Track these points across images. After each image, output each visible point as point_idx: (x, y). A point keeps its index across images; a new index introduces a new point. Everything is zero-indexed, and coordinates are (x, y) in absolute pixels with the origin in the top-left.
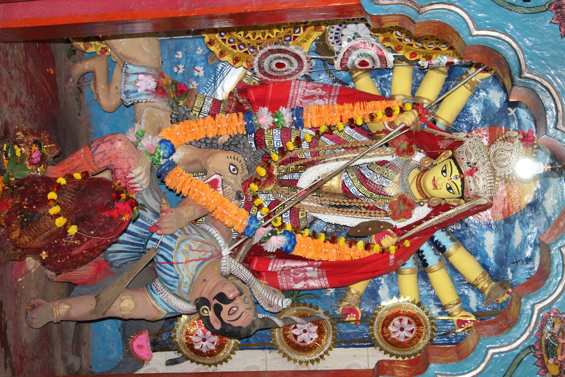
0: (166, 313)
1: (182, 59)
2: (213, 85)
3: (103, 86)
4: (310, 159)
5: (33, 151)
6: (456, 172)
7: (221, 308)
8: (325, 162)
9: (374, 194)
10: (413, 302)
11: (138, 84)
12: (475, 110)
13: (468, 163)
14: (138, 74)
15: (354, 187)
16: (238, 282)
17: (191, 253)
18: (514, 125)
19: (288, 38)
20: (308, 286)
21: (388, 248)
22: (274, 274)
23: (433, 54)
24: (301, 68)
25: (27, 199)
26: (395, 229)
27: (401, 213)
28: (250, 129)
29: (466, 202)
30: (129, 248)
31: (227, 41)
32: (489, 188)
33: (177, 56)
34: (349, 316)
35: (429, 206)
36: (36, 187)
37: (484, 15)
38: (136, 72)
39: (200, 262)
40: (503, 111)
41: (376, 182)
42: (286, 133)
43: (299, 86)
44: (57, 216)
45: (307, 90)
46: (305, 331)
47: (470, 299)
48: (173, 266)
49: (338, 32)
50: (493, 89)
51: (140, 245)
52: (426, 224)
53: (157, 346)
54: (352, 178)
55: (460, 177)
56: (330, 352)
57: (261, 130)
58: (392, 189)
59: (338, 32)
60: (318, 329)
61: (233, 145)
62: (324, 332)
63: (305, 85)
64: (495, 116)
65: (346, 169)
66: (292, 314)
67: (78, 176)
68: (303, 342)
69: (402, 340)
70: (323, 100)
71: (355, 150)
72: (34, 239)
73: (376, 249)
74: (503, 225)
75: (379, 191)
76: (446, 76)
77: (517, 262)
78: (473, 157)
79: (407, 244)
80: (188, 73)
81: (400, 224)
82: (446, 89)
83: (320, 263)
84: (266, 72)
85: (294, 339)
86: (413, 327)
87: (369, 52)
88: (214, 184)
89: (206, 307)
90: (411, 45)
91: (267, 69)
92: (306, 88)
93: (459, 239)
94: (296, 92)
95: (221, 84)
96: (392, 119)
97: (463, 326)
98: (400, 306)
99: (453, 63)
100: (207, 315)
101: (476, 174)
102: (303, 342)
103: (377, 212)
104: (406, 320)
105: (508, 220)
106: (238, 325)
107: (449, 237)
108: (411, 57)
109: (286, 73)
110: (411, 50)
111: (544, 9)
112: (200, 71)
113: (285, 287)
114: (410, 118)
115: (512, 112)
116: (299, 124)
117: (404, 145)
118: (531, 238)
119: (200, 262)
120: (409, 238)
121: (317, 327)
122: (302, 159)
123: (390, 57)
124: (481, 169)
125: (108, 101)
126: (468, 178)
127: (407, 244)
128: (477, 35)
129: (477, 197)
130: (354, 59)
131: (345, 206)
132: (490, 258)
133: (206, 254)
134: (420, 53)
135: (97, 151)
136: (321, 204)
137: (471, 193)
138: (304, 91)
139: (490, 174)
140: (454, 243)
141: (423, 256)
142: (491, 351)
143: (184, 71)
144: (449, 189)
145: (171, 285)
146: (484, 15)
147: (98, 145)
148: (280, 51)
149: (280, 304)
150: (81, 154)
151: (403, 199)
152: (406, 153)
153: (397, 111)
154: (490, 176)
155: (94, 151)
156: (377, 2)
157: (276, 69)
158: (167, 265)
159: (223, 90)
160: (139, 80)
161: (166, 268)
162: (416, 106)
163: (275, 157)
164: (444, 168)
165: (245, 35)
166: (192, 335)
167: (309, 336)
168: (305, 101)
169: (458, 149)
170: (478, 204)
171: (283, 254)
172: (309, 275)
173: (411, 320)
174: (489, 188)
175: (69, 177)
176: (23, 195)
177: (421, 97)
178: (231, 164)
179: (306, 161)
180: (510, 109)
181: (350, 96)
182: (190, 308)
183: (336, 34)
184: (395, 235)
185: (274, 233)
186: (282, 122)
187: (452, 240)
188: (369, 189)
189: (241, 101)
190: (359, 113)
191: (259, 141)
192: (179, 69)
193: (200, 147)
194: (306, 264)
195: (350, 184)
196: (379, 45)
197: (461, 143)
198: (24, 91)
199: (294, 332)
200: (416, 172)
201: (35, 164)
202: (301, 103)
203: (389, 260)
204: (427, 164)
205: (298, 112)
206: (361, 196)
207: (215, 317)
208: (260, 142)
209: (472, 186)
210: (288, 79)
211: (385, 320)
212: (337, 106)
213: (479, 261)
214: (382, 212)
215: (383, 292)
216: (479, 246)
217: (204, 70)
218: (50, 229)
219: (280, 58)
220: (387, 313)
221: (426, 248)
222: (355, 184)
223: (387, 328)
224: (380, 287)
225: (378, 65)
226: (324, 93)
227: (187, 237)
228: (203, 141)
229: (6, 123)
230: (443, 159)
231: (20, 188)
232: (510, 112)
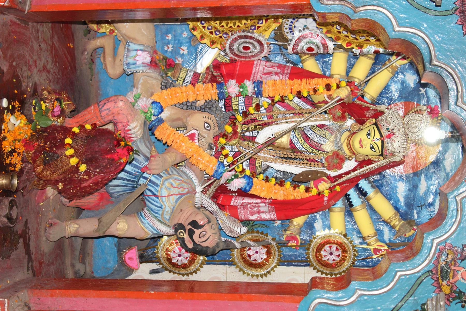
0: (151, 234)
2: (194, 61)
3: (110, 59)
5: (55, 106)
7: (194, 232)
8: (277, 124)
9: (314, 150)
11: (136, 58)
12: (395, 89)
13: (387, 129)
14: (137, 50)
16: (207, 213)
17: (172, 189)
18: (424, 101)
19: (253, 28)
20: (261, 218)
21: (323, 191)
22: (235, 207)
23: (364, 44)
25: (49, 143)
26: (329, 177)
27: (334, 165)
28: (221, 96)
29: (384, 159)
30: (126, 183)
31: (206, 28)
32: (403, 149)
33: (167, 38)
34: (291, 242)
35: (356, 161)
36: (56, 134)
37: (405, 16)
39: (179, 196)
40: (416, 90)
41: (316, 140)
42: (248, 100)
43: (260, 64)
44: (72, 156)
45: (266, 68)
46: (257, 252)
47: (385, 233)
49: (291, 24)
50: (408, 72)
51: (133, 181)
52: (353, 174)
53: (143, 259)
55: (381, 139)
56: (275, 269)
57: (230, 97)
58: (328, 147)
59: (291, 24)
60: (267, 251)
61: (207, 107)
62: (271, 254)
63: (264, 64)
64: (409, 94)
65: (293, 129)
66: (247, 239)
67: (88, 127)
69: (331, 262)
71: (301, 115)
72: (53, 173)
73: (314, 192)
74: (412, 177)
75: (318, 148)
76: (374, 62)
77: (421, 206)
78: (392, 125)
79: (338, 189)
80: (176, 52)
82: (372, 71)
83: (270, 201)
84: (235, 53)
85: (248, 258)
86: (340, 252)
87: (315, 41)
88: (192, 137)
89: (182, 231)
90: (348, 37)
91: (236, 51)
92: (266, 66)
93: (378, 187)
94: (257, 69)
96: (330, 93)
97: (378, 253)
98: (330, 236)
99: (379, 51)
101: (393, 137)
102: (255, 260)
103: (316, 163)
104: (334, 247)
105: (416, 174)
106: (206, 246)
107: (370, 185)
108: (347, 46)
109: (250, 54)
110: (347, 40)
111: (451, 13)
112: (184, 50)
113: (243, 218)
114: (344, 93)
115: (423, 91)
116: (259, 94)
117: (339, 113)
118: (433, 188)
119: (179, 196)
120: (339, 185)
121: (266, 249)
122: (260, 120)
123: (331, 45)
124: (397, 134)
125: (113, 70)
126: (387, 140)
127: (338, 189)
128: (399, 31)
129: (393, 155)
130: (303, 45)
131: (291, 158)
132: (401, 202)
134: (354, 43)
135: (103, 109)
136: (273, 156)
138: (264, 69)
139: (404, 138)
140: (374, 190)
141: (350, 199)
142: (399, 274)
143: (172, 50)
144: (372, 148)
145: (156, 213)
146: (405, 16)
147: (105, 104)
148: (246, 37)
149: (239, 231)
150: (92, 110)
151: (336, 154)
152: (340, 119)
153: (335, 86)
154: (404, 139)
156: (322, 2)
157: (243, 51)
158: (154, 198)
159: (202, 65)
160: (137, 55)
161: (153, 200)
162: (349, 83)
163: (240, 118)
164: (369, 132)
165: (220, 24)
166: (170, 251)
167: (260, 256)
168: (264, 76)
169: (380, 118)
170: (393, 160)
171: (242, 193)
172: (261, 209)
173: (338, 247)
174: (403, 149)
175: (82, 127)
176: (46, 139)
177: (353, 77)
179: (263, 122)
180: (421, 89)
181: (298, 73)
182: (170, 231)
183: (290, 25)
184: (329, 182)
185: (236, 176)
186: (246, 92)
189: (215, 74)
190: (305, 87)
191: (228, 105)
192: (168, 48)
193: (182, 109)
194: (259, 201)
195: (296, 141)
196: (323, 35)
197: (382, 113)
198: (50, 60)
199: (249, 252)
200: (347, 134)
201: (56, 116)
202: (261, 77)
203: (323, 201)
204: (356, 128)
205: (259, 84)
206: (304, 151)
208: (228, 107)
209: (390, 146)
210: (252, 59)
211: (319, 246)
212: (288, 81)
213: (392, 204)
215: (318, 225)
216: (393, 193)
217: (187, 49)
218: (66, 166)
219: (246, 42)
220: (320, 241)
221: (352, 193)
222: (300, 141)
223: (320, 252)
224: (316, 221)
225: (322, 51)
226: (279, 71)
227: (170, 176)
228: (184, 104)
229: (35, 84)
231: (44, 134)
232: (421, 91)
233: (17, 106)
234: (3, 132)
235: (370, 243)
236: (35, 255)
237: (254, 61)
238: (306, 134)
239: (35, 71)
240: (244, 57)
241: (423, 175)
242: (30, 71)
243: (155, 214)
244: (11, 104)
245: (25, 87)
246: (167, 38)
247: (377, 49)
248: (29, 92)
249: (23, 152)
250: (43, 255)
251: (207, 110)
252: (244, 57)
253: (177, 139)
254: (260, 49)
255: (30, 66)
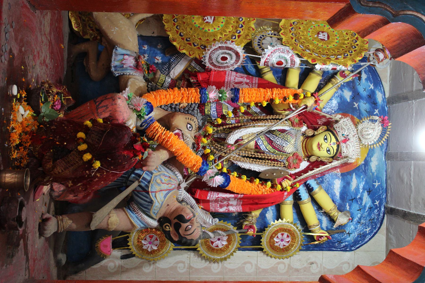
0: (140, 227)
1: (147, 50)
3: (93, 63)
4: (236, 125)
6: (334, 140)
7: (180, 226)
8: (246, 127)
9: (277, 151)
10: (292, 223)
11: (123, 62)
13: (342, 135)
14: (124, 55)
15: (263, 146)
17: (163, 185)
20: (229, 210)
21: (286, 188)
22: (208, 201)
24: (237, 61)
25: (58, 137)
26: (291, 175)
33: (144, 48)
35: (308, 161)
36: (66, 128)
38: (122, 53)
39: (167, 191)
41: (278, 143)
44: (85, 152)
45: (236, 78)
46: (219, 239)
48: (149, 194)
49: (259, 41)
53: (116, 245)
54: (262, 139)
55: (337, 143)
56: (234, 253)
58: (289, 148)
59: (259, 41)
60: (228, 238)
62: (232, 240)
63: (235, 75)
68: (217, 246)
69: (281, 247)
70: (248, 85)
73: (279, 187)
75: (280, 150)
77: (352, 200)
78: (346, 131)
81: (293, 172)
83: (242, 196)
84: (213, 63)
85: (211, 244)
87: (286, 56)
89: (168, 224)
90: (312, 54)
91: (214, 61)
92: (236, 76)
94: (229, 79)
95: (173, 70)
96: (297, 101)
98: (283, 225)
100: (169, 230)
101: (348, 142)
104: (286, 234)
106: (190, 238)
109: (225, 65)
114: (310, 102)
117: (297, 120)
119: (167, 191)
122: (229, 124)
124: (352, 140)
126: (343, 145)
132: (337, 196)
133: (171, 186)
134: (319, 60)
135: (100, 106)
136: (239, 155)
137: (343, 155)
138: (235, 79)
139: (357, 143)
141: (299, 193)
143: (148, 59)
147: (102, 101)
149: (211, 222)
151: (295, 155)
153: (302, 97)
155: (99, 105)
158: (144, 193)
159: (174, 74)
160: (124, 59)
161: (142, 195)
164: (325, 137)
166: (142, 239)
167: (221, 243)
169: (335, 126)
171: (221, 189)
172: (230, 203)
173: (289, 235)
175: (94, 121)
177: (306, 90)
178: (188, 123)
179: (233, 125)
180: (355, 103)
183: (259, 42)
184: (292, 179)
186: (224, 97)
187: (318, 184)
188: (274, 147)
193: (167, 110)
194: (233, 196)
195: (261, 143)
198: (48, 55)
200: (302, 138)
203: (284, 196)
204: (310, 133)
205: (236, 91)
206: (267, 152)
207: (175, 232)
210: (226, 69)
211: (273, 234)
213: (331, 197)
214: (282, 163)
216: (331, 188)
217: (161, 59)
218: (77, 162)
226: (248, 81)
227: (159, 173)
228: (169, 106)
229: (38, 75)
230: (321, 131)
231: (52, 128)
232: (355, 105)
233: (23, 95)
234: (11, 122)
235: (315, 231)
236: (31, 253)
237: (225, 72)
238: (268, 137)
239: (38, 62)
240: (219, 67)
241: (354, 174)
242: (34, 61)
243: (144, 209)
244: (19, 93)
245: (30, 77)
246: (144, 48)
247: (335, 67)
248: (33, 83)
249: (30, 146)
250: (36, 252)
251: (190, 112)
252: (219, 67)
253: (172, 138)
254: (236, 61)
255: (34, 56)
